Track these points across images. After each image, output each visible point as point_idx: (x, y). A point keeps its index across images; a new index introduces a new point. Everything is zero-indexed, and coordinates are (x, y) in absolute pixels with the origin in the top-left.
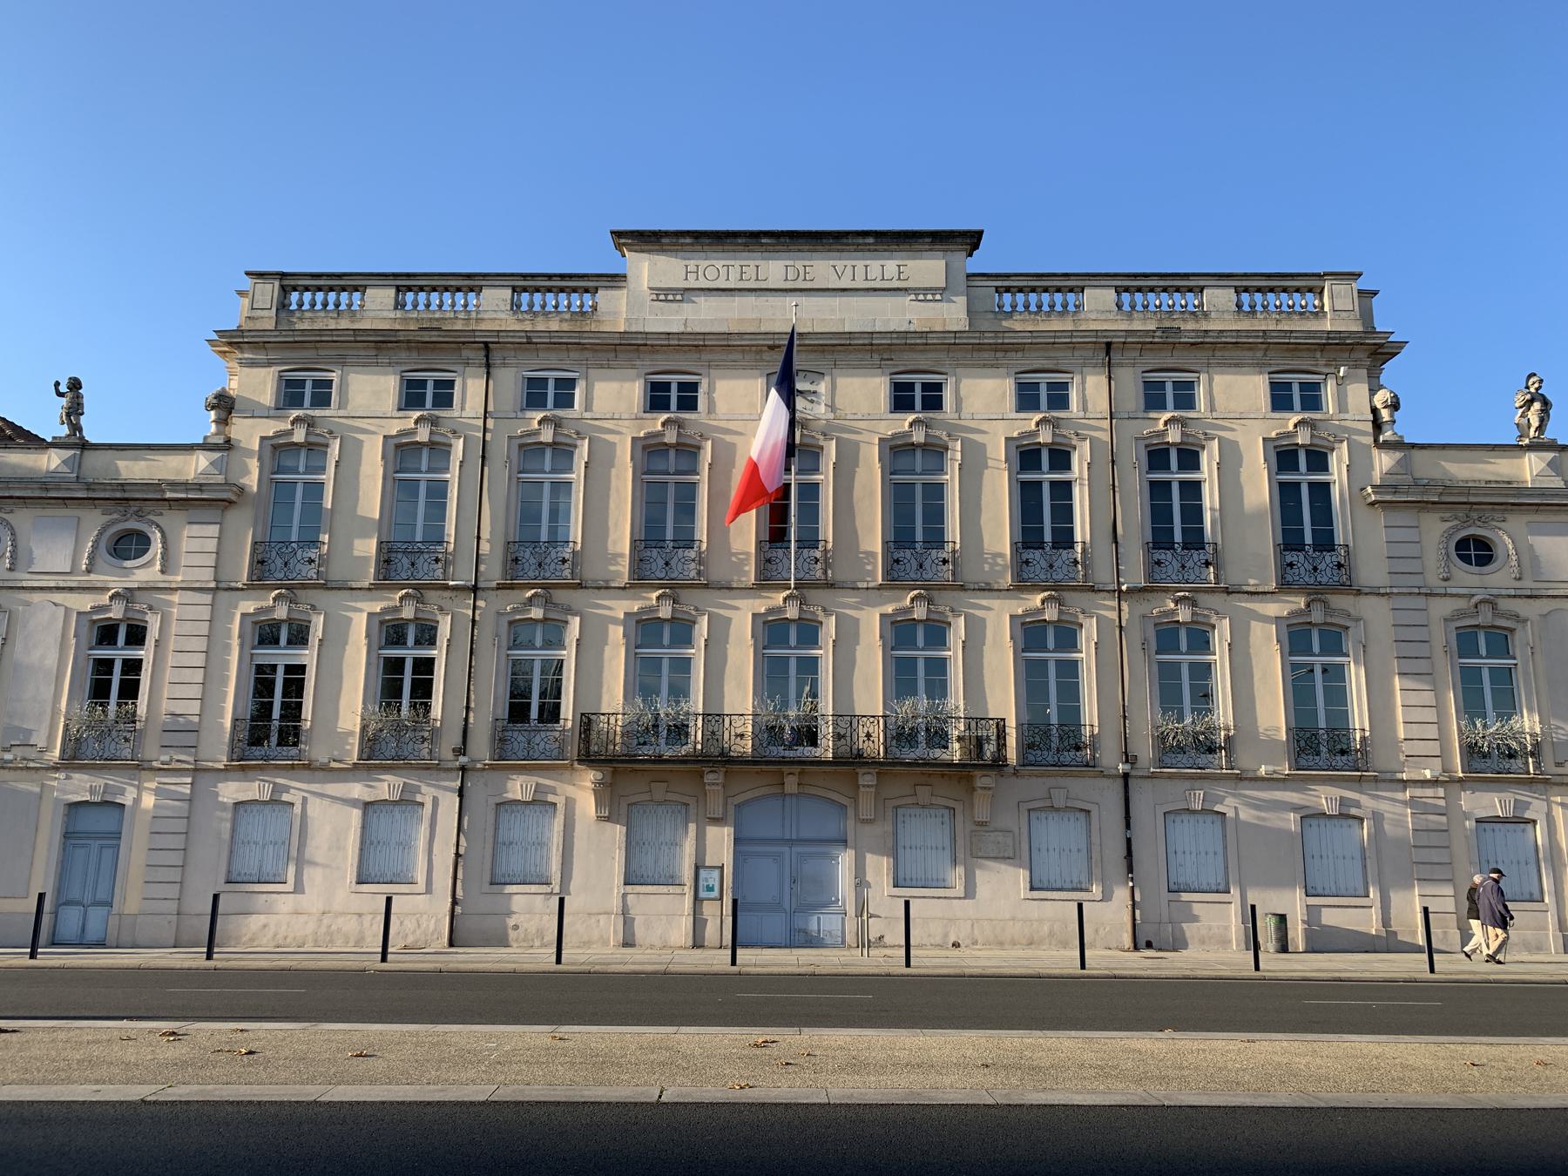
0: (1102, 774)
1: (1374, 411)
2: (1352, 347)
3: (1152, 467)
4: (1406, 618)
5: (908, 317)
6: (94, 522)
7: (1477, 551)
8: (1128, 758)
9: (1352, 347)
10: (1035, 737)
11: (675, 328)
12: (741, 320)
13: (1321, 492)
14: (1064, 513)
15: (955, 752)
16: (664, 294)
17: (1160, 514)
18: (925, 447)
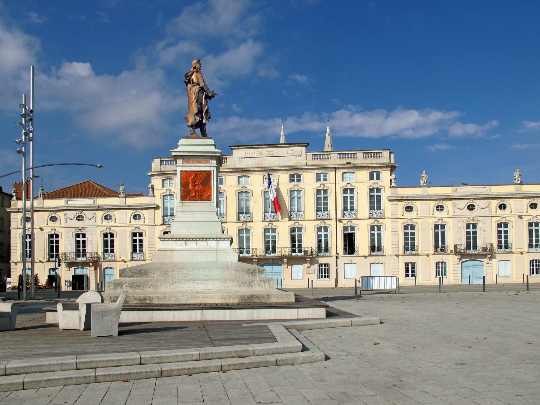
0: (332, 257)
1: (391, 180)
2: (386, 167)
3: (344, 193)
4: (393, 223)
5: (293, 162)
6: (130, 213)
7: (409, 209)
8: (337, 253)
9: (386, 167)
10: (319, 250)
11: (244, 166)
12: (258, 164)
13: (379, 197)
14: (326, 204)
15: (302, 254)
16: (241, 159)
17: (345, 203)
18: (297, 190)
